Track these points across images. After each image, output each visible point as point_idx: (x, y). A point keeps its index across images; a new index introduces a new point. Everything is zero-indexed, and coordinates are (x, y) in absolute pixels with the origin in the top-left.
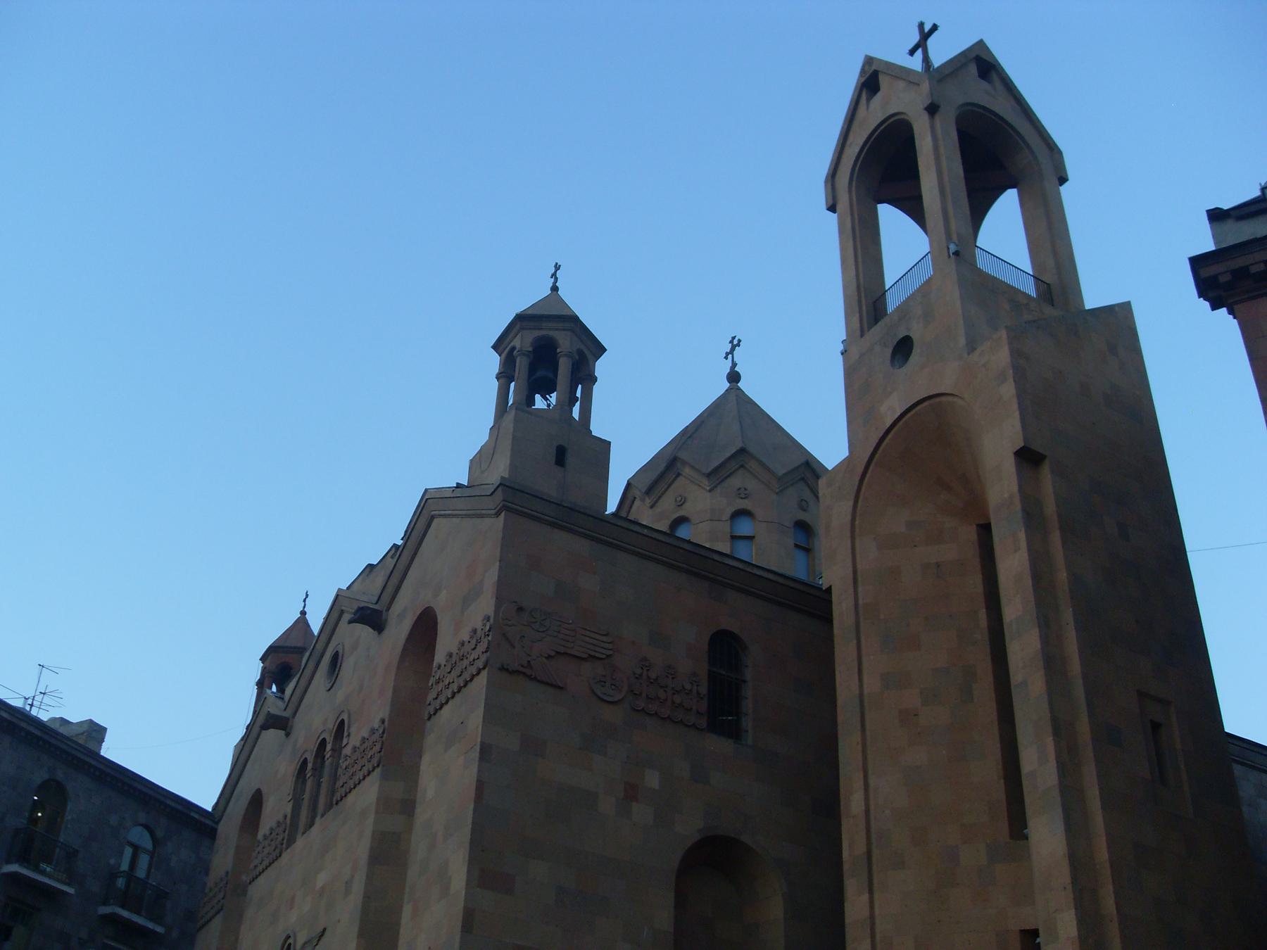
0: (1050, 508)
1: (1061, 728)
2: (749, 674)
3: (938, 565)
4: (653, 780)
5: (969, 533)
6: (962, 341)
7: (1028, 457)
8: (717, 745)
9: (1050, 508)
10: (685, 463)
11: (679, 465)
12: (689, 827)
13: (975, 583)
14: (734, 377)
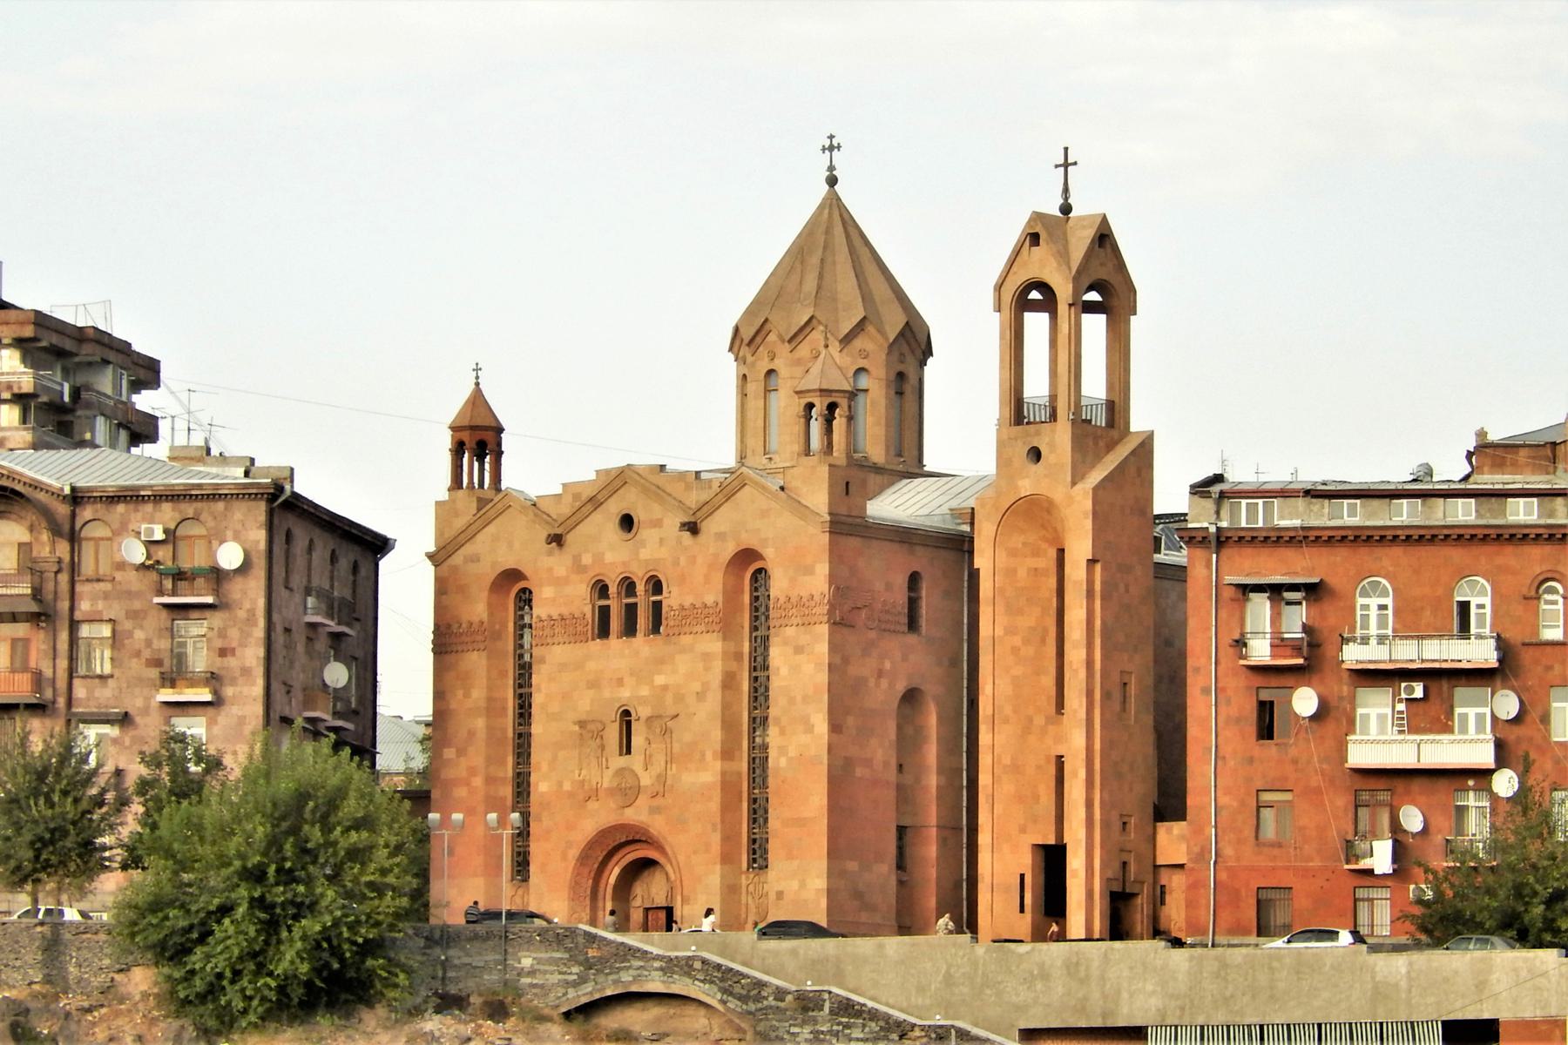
0: (1098, 586)
1: (1090, 694)
2: (924, 593)
3: (1036, 569)
4: (888, 665)
5: (1052, 553)
6: (1069, 479)
7: (1092, 562)
8: (912, 639)
9: (1098, 586)
10: (820, 322)
11: (814, 321)
12: (901, 687)
13: (1052, 582)
14: (832, 181)
